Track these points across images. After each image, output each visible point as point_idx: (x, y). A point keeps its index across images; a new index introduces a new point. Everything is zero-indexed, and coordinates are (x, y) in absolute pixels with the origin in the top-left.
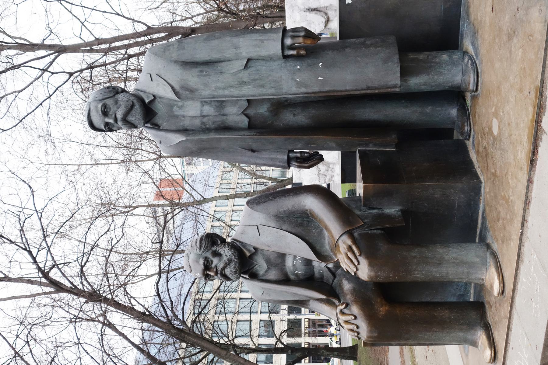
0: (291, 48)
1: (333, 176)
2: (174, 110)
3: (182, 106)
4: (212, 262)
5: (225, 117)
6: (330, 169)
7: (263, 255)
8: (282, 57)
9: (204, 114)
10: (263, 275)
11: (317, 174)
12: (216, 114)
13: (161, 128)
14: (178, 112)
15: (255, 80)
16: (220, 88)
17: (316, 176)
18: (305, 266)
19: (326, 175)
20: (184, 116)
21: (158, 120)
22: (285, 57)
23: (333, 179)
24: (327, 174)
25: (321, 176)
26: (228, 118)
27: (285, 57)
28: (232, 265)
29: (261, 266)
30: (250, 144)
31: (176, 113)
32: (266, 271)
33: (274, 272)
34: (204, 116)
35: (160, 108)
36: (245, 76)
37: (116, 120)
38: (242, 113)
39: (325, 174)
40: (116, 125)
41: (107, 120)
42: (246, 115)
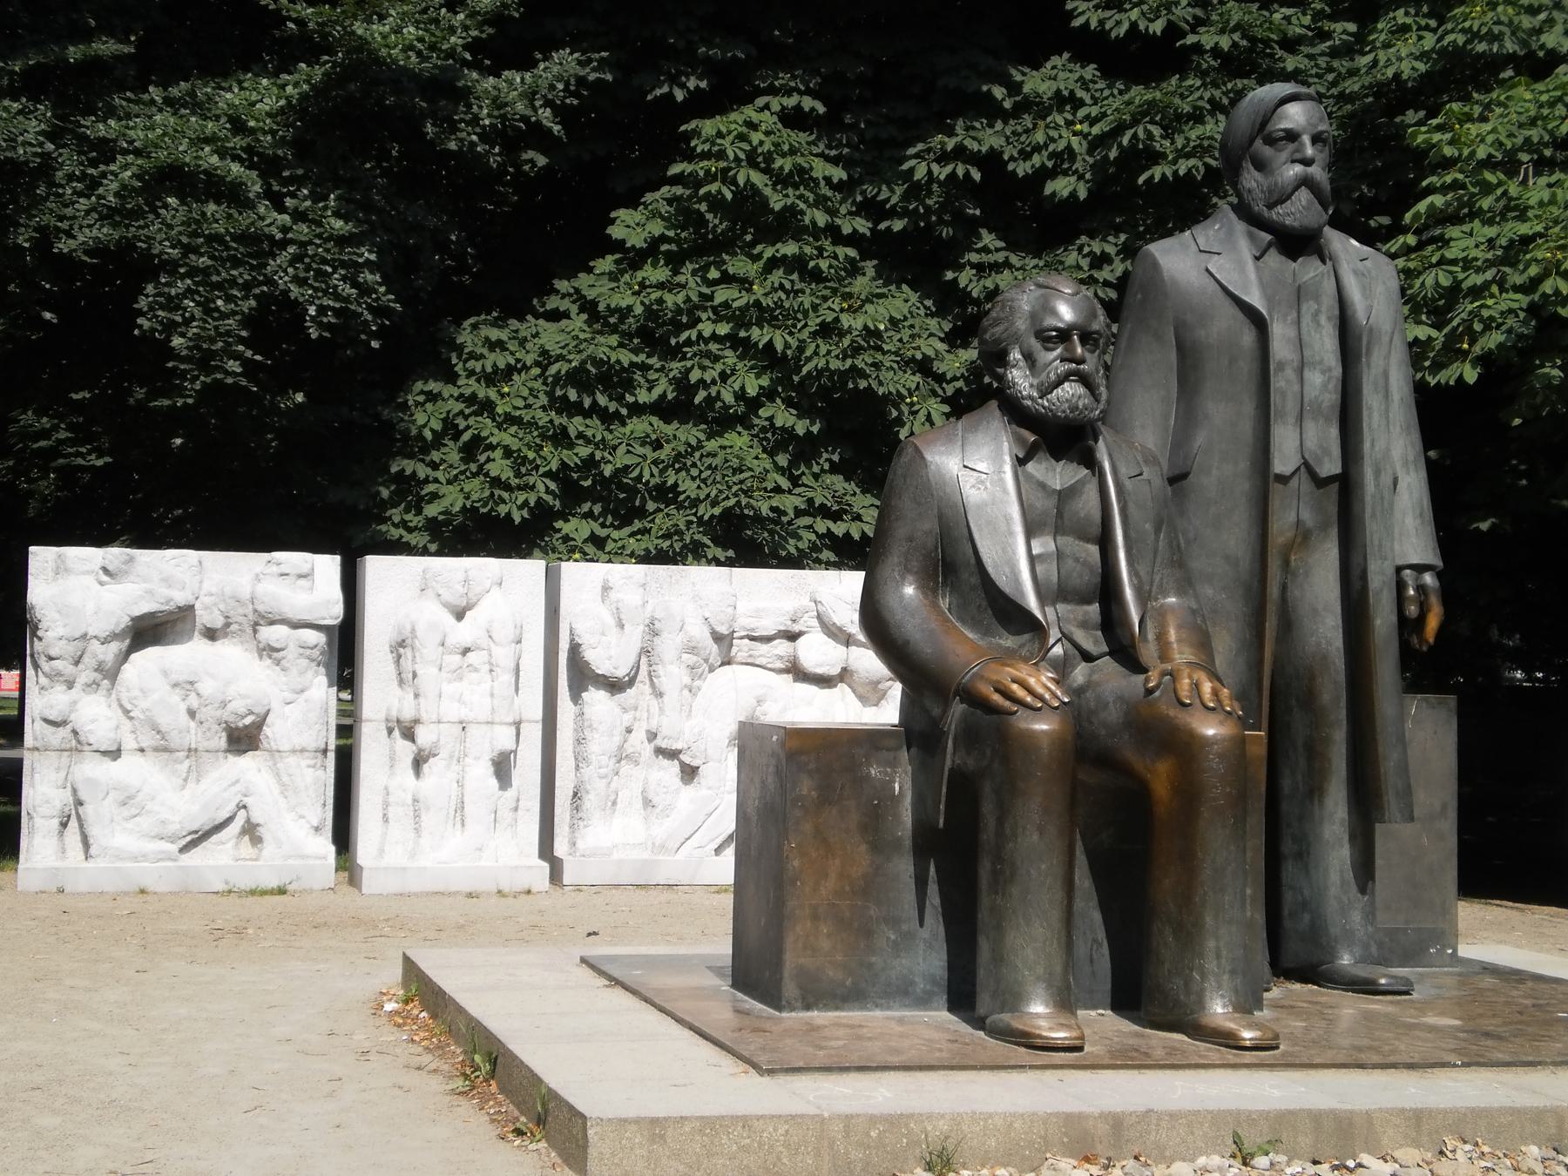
0: (1421, 588)
1: (70, 685)
2: (1311, 302)
3: (1318, 324)
4: (1092, 352)
5: (1291, 419)
6: (98, 676)
7: (1081, 482)
8: (1401, 562)
9: (1307, 374)
10: (1029, 477)
11: (91, 632)
12: (1306, 400)
13: (1260, 263)
14: (1308, 307)
15: (1382, 498)
16: (1370, 417)
17: (82, 631)
18: (1059, 586)
19: (77, 663)
20: (1298, 322)
21: (1274, 259)
22: (1399, 569)
23: (60, 688)
24: (81, 666)
25: (79, 644)
26: (1290, 427)
27: (1399, 569)
28: (1087, 400)
29: (1057, 474)
30: (1214, 472)
31: (1304, 308)
32: (1042, 486)
33: (1038, 505)
34: (1300, 371)
35: (1309, 269)
36: (1386, 480)
37: (1307, 162)
38: (1306, 464)
39: (86, 659)
40: (1284, 155)
41: (1306, 139)
42: (1298, 469)
